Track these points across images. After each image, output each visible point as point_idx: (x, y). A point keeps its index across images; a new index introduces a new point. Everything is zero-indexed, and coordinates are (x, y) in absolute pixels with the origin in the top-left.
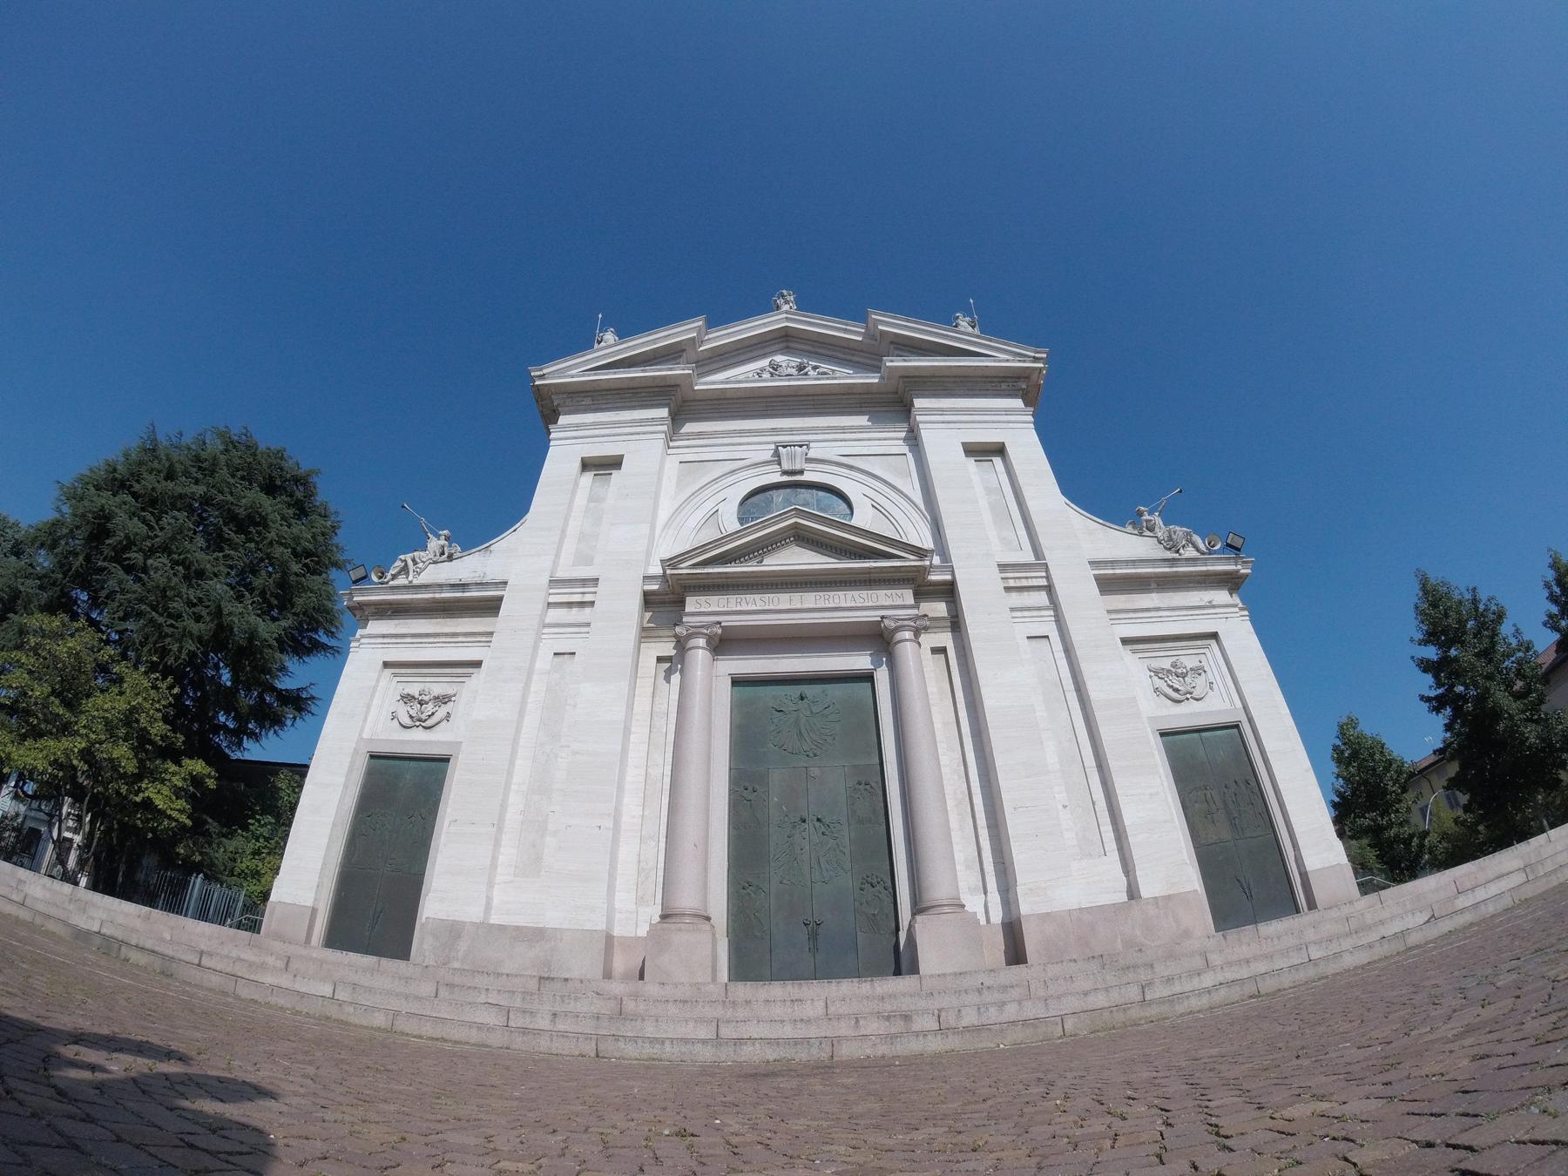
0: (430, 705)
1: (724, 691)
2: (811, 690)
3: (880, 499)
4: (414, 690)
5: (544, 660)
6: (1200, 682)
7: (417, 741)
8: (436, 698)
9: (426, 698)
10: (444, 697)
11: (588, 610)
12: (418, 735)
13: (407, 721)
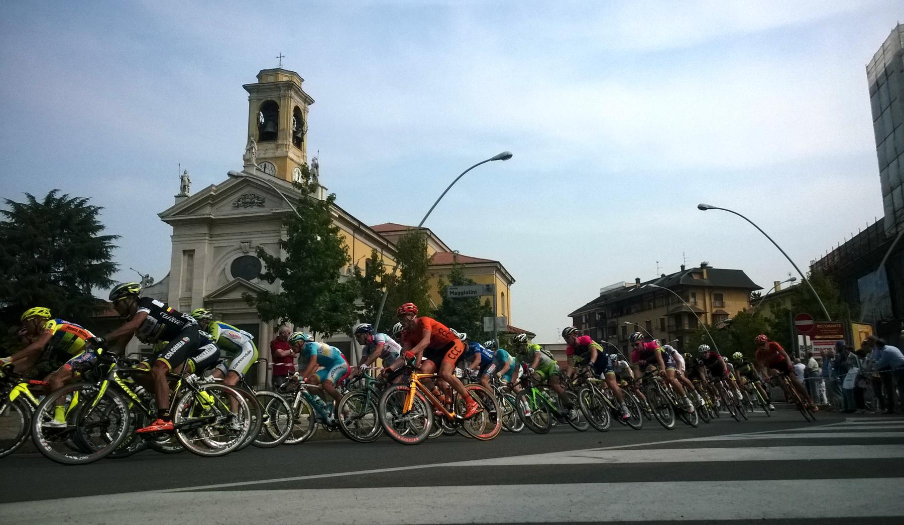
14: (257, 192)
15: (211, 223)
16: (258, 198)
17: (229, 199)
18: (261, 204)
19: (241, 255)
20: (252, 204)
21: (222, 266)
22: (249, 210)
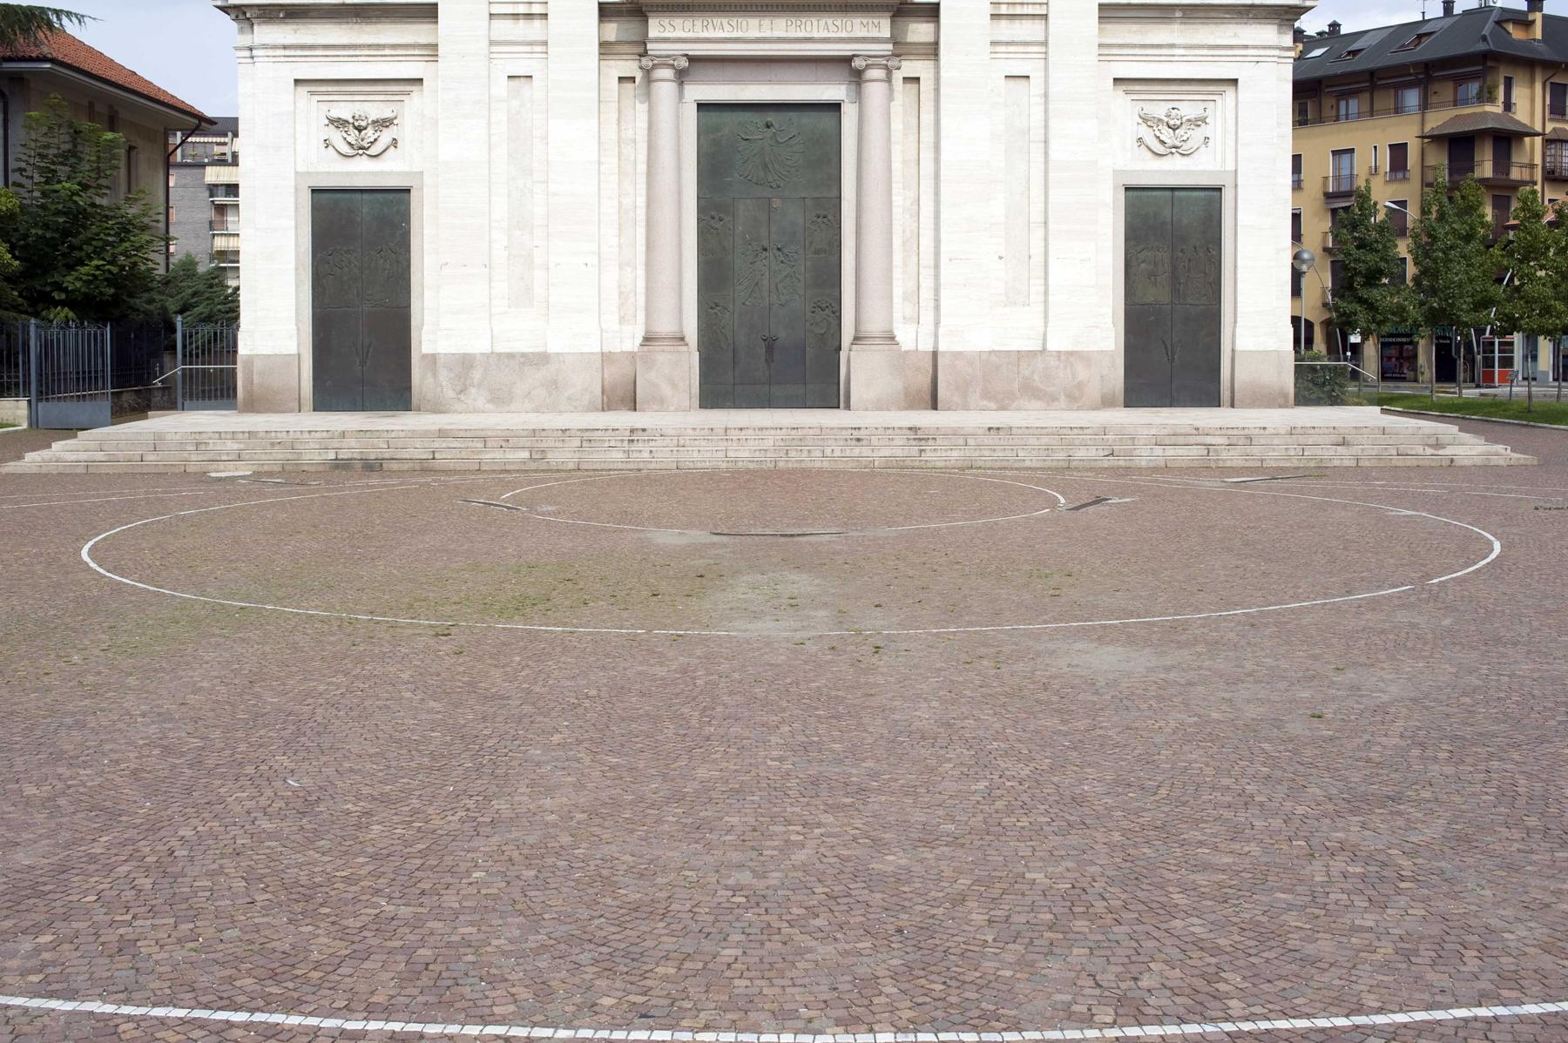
1: (691, 115)
2: (771, 117)
4: (344, 111)
5: (501, 87)
6: (1197, 135)
8: (374, 122)
9: (363, 124)
10: (384, 121)
11: (537, 23)
13: (346, 149)
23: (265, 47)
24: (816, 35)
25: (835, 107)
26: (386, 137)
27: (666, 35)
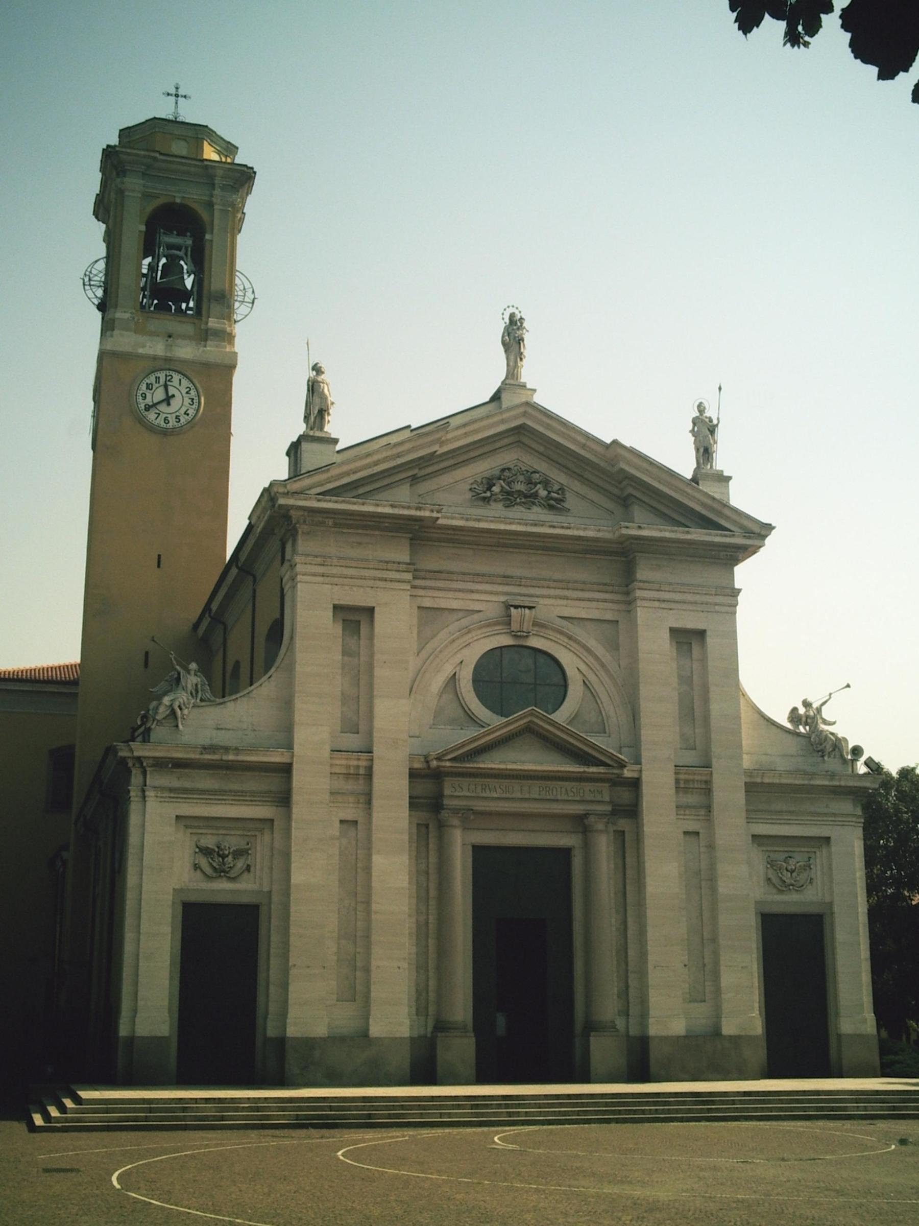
0: (230, 858)
3: (591, 677)
4: (209, 842)
7: (223, 890)
12: (223, 885)
13: (209, 870)
14: (542, 466)
15: (418, 533)
16: (546, 483)
17: (459, 474)
18: (555, 504)
19: (506, 640)
20: (530, 499)
21: (448, 670)
22: (518, 512)
23: (155, 788)
24: (559, 797)
25: (566, 853)
26: (240, 864)
27: (456, 794)
